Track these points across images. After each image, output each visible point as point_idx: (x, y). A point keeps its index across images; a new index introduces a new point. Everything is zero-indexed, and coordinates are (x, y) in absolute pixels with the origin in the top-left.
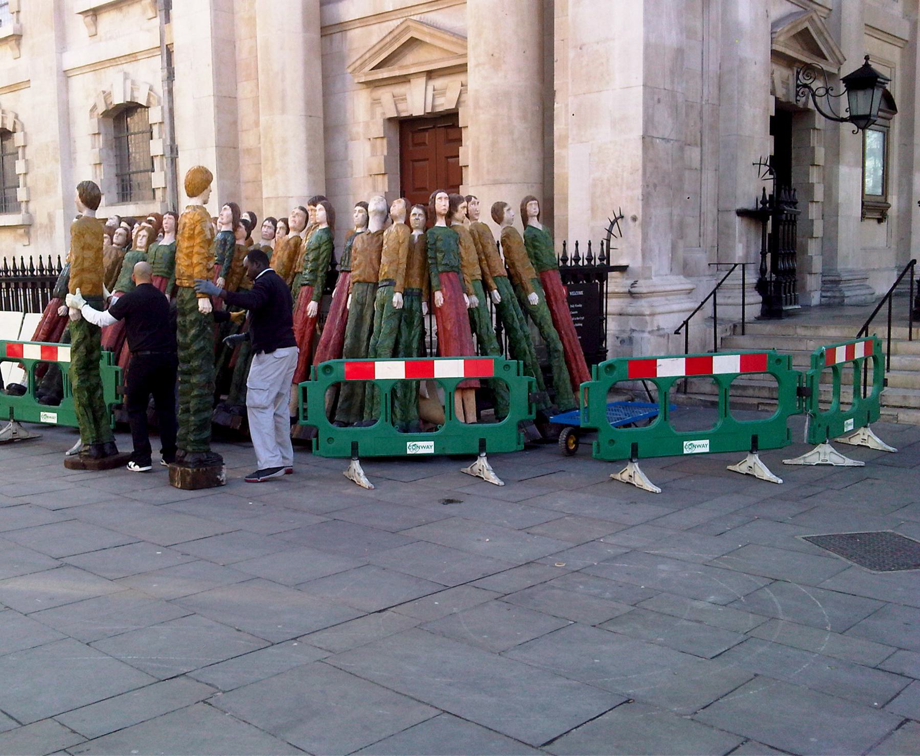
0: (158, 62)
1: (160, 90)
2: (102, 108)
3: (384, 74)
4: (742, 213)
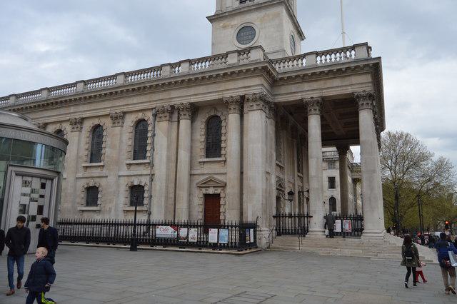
0: (148, 178)
1: (148, 183)
3: (204, 185)
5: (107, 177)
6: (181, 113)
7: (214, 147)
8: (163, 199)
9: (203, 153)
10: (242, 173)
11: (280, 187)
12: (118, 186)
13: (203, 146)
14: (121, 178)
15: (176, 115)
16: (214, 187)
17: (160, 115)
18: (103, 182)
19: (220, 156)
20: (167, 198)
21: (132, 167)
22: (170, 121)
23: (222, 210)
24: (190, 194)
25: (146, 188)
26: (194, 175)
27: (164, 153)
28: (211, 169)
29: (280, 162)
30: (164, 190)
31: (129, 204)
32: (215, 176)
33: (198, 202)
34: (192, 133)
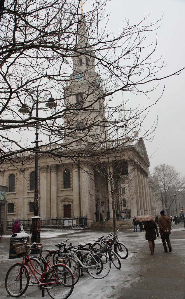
2: (29, 202)
4: (95, 213)
5: (18, 198)
6: (52, 169)
7: (67, 183)
8: (45, 208)
9: (62, 186)
10: (80, 195)
11: (97, 200)
12: (24, 203)
13: (62, 183)
14: (25, 199)
15: (49, 170)
16: (68, 201)
17: (43, 170)
18: (16, 201)
19: (70, 188)
20: (47, 207)
21: (30, 194)
22: (47, 172)
23: (72, 211)
24: (57, 205)
26: (59, 196)
27: (45, 187)
28: (66, 193)
29: (97, 188)
30: (46, 204)
31: (29, 211)
33: (61, 208)
34: (57, 178)
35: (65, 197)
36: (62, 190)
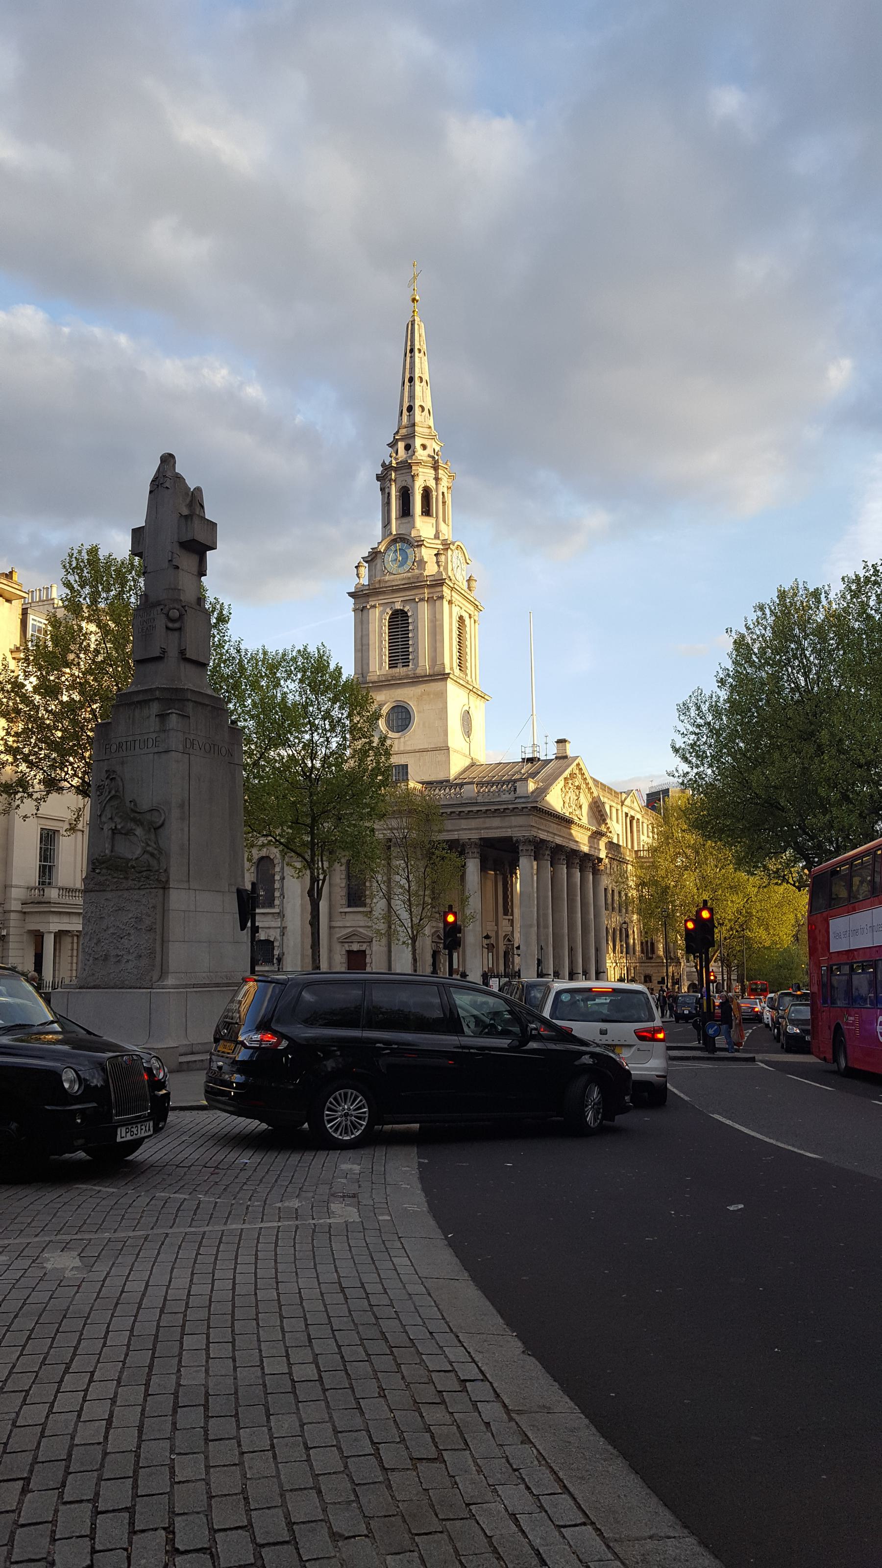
1: (279, 938)
8: (299, 957)
13: (344, 892)
19: (365, 905)
24: (330, 950)
25: (276, 944)
32: (361, 930)
35: (350, 930)
36: (342, 910)
